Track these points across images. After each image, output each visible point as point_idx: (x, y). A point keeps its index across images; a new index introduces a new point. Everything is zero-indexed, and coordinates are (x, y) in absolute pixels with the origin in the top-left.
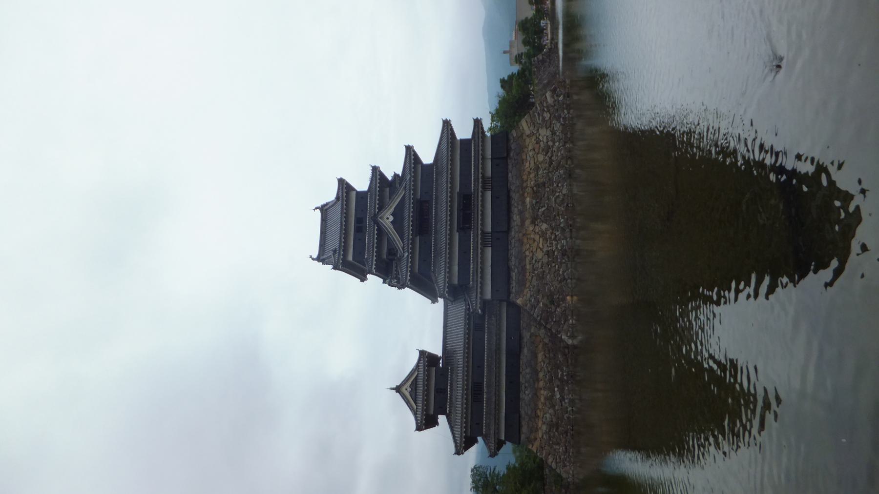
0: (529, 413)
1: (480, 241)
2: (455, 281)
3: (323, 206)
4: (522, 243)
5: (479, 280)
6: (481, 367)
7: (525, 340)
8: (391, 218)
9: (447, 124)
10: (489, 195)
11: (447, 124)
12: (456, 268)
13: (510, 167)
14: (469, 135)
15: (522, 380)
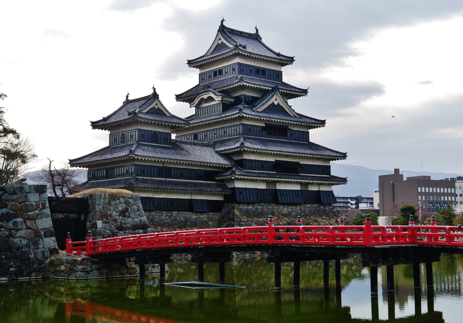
0: (155, 220)
1: (276, 179)
2: (246, 157)
3: (259, 36)
4: (273, 214)
5: (252, 178)
6: (181, 177)
7: (201, 217)
8: (276, 103)
9: (344, 156)
10: (298, 188)
11: (344, 156)
12: (253, 157)
13: (314, 206)
14: (333, 173)
15: (175, 213)
